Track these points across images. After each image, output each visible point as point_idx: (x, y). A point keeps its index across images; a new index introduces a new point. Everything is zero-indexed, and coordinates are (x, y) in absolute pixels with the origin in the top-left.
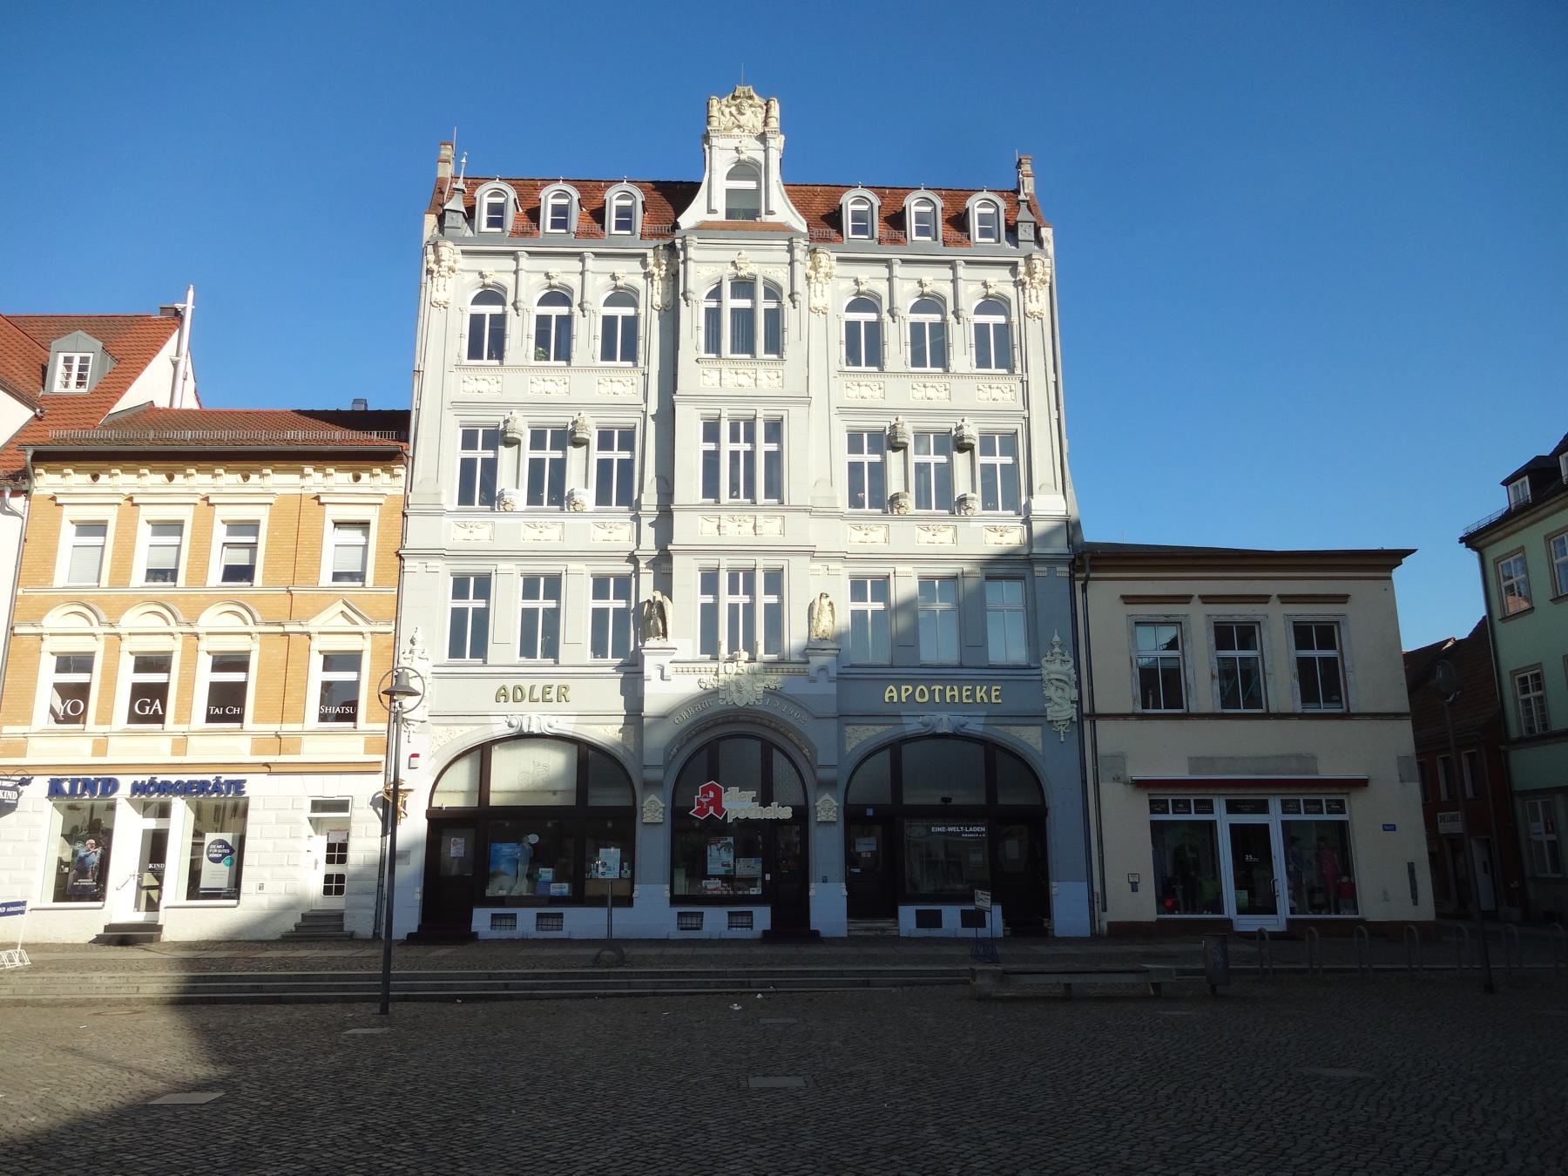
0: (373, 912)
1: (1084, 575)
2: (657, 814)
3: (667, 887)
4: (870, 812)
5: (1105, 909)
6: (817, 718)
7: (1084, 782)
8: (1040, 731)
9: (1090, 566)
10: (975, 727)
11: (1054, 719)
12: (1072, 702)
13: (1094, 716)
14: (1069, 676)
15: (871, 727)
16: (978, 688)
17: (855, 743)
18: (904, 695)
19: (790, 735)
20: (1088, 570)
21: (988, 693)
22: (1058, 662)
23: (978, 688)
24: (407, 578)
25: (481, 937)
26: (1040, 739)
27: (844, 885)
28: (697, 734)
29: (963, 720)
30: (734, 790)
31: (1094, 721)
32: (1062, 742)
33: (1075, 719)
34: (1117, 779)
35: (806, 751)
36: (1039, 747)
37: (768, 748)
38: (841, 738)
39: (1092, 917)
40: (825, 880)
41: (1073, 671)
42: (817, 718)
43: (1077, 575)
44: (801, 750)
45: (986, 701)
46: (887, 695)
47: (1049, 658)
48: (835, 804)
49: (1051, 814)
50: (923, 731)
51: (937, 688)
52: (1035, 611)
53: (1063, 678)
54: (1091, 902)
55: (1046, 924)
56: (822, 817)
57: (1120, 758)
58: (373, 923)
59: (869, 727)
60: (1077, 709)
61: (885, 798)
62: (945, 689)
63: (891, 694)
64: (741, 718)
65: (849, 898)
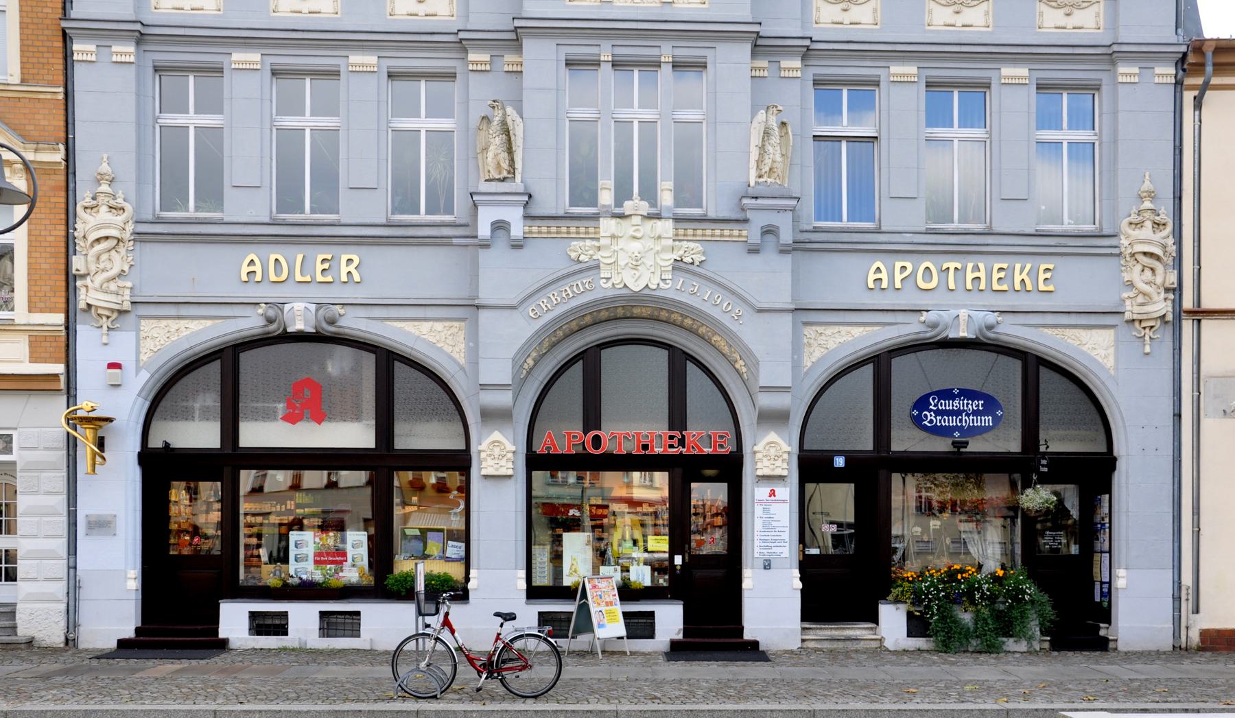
0: (63, 607)
1: (1199, 81)
2: (503, 462)
3: (522, 574)
4: (840, 462)
5: (1197, 610)
6: (760, 311)
7: (1178, 416)
8: (1112, 338)
9: (1215, 65)
11: (1135, 317)
12: (1167, 290)
13: (1199, 314)
14: (1164, 247)
15: (844, 329)
16: (1018, 267)
17: (818, 353)
19: (715, 338)
20: (1209, 69)
21: (1033, 274)
22: (1148, 224)
23: (1018, 267)
24: (79, 73)
25: (232, 645)
26: (1112, 350)
27: (796, 573)
28: (566, 336)
29: (992, 318)
31: (1199, 321)
32: (1147, 354)
33: (1170, 317)
35: (740, 364)
36: (1110, 363)
37: (679, 360)
38: (797, 347)
39: (1177, 620)
40: (767, 566)
41: (1170, 241)
42: (760, 311)
43: (1189, 81)
44: (732, 363)
45: (1029, 287)
46: (872, 277)
47: (1134, 218)
48: (786, 448)
49: (1121, 465)
50: (928, 335)
51: (952, 265)
52: (1115, 141)
53: (1158, 251)
54: (1177, 599)
55: (1102, 633)
56: (764, 468)
58: (63, 624)
59: (842, 328)
60: (1174, 301)
61: (865, 442)
62: (964, 269)
63: (878, 276)
64: (636, 311)
65: (804, 593)
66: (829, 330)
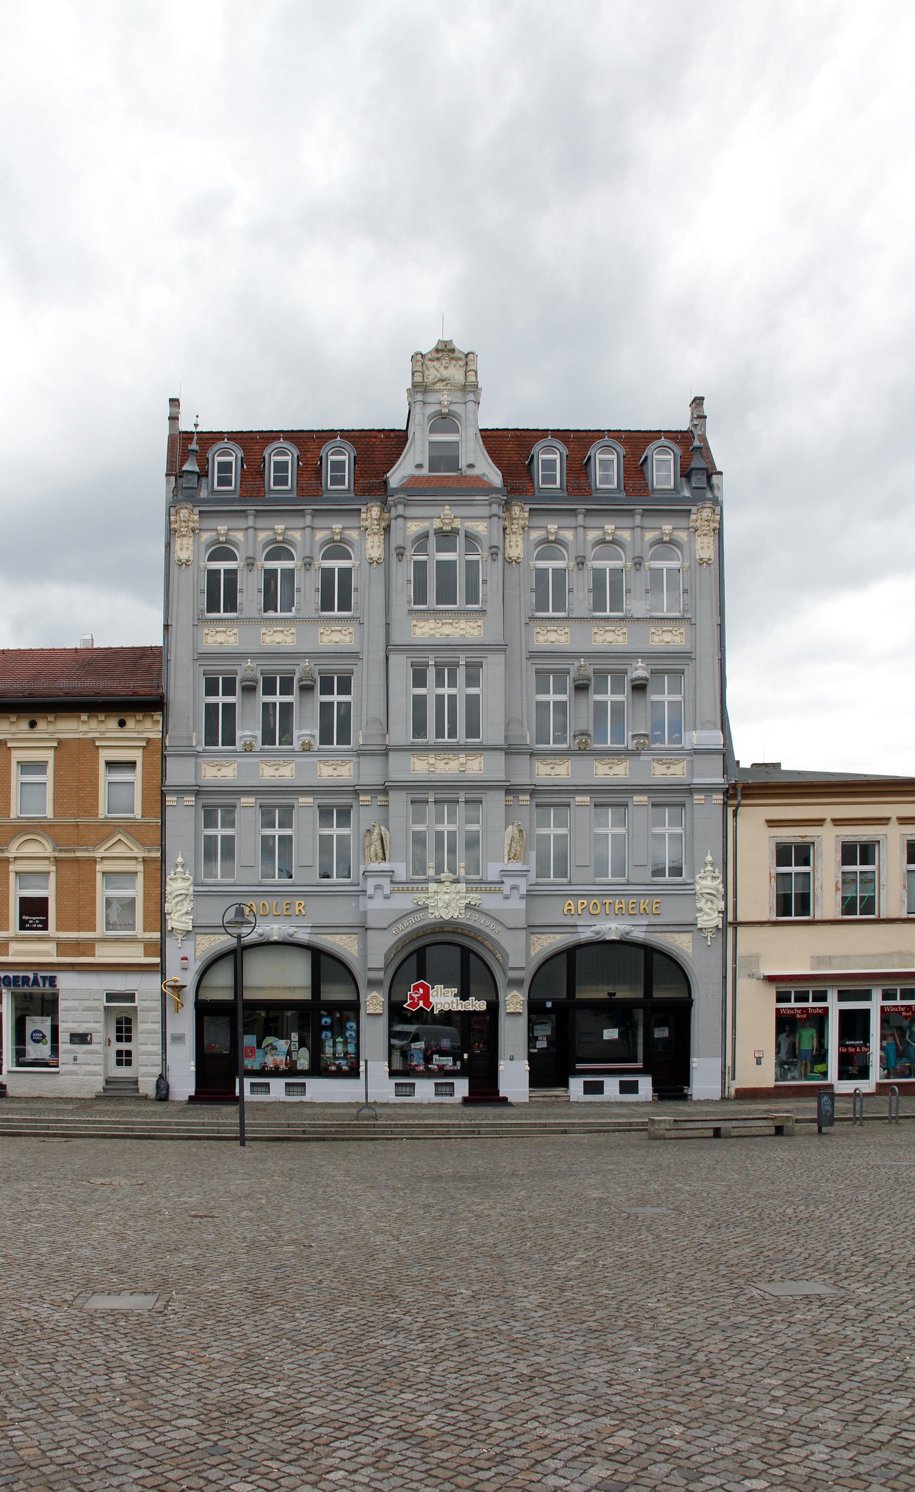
4: (549, 1005)
5: (733, 1078)
10: (638, 935)
13: (736, 924)
18: (580, 908)
29: (628, 928)
30: (439, 987)
33: (720, 926)
34: (751, 976)
39: (723, 1084)
40: (512, 1059)
54: (723, 1073)
57: (755, 959)
66: (544, 937)
